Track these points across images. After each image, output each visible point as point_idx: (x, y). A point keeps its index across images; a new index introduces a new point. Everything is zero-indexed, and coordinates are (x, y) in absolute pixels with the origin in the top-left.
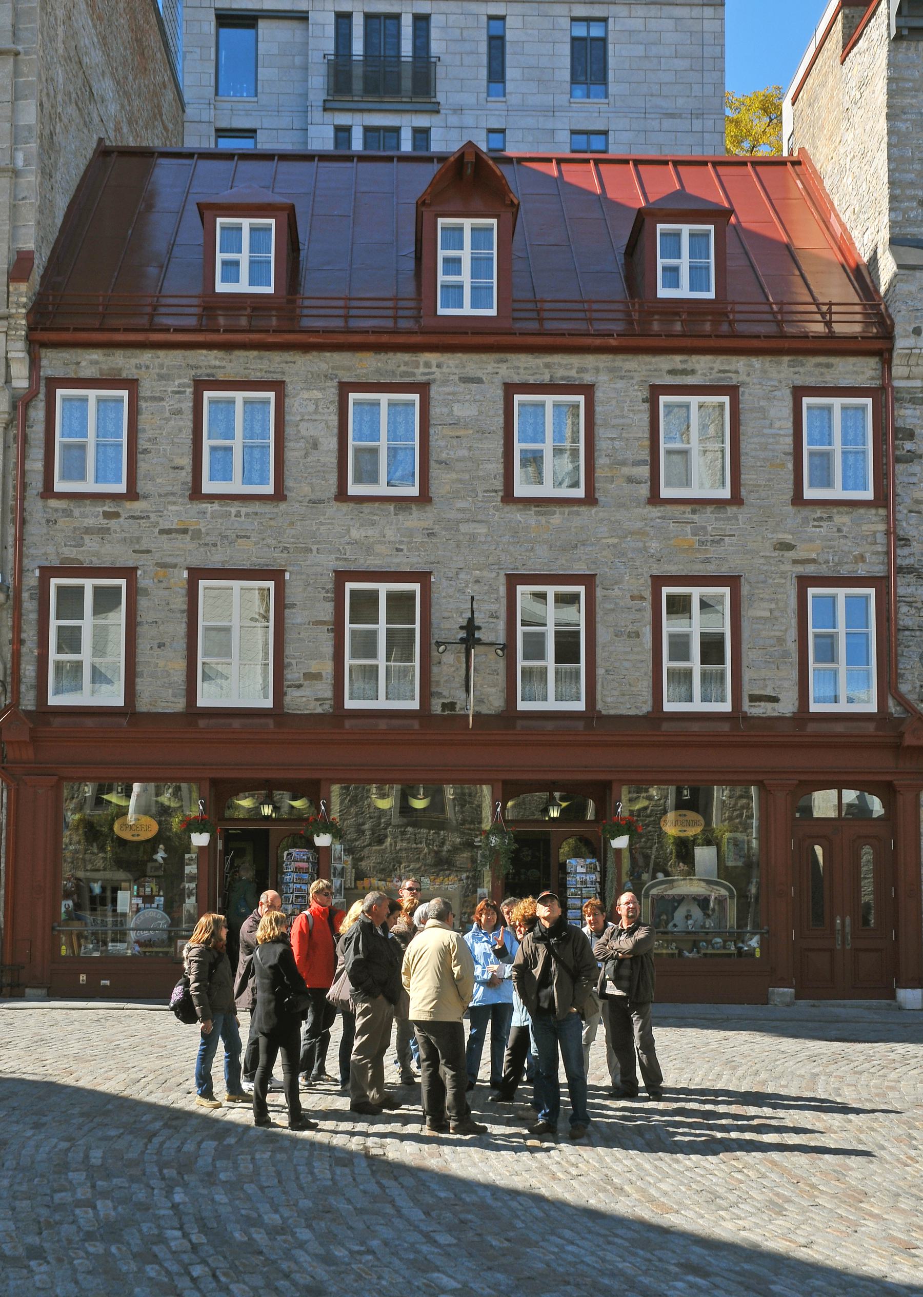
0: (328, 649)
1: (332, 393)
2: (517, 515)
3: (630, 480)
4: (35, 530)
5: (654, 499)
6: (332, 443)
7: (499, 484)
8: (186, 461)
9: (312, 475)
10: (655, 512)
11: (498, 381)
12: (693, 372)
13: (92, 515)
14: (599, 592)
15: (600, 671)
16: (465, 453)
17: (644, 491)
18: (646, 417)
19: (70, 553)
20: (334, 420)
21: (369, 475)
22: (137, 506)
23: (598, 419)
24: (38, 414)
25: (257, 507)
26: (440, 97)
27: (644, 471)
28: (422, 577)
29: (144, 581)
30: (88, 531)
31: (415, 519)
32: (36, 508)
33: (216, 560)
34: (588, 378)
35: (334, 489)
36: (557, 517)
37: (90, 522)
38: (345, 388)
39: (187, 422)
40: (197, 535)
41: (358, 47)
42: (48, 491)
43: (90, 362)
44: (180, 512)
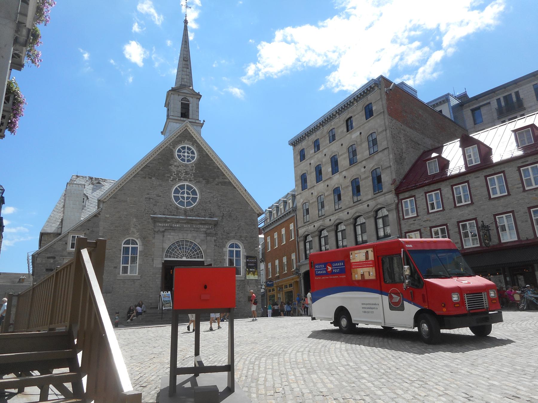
0: (459, 237)
1: (450, 187)
2: (493, 202)
3: (518, 188)
4: (403, 226)
5: (524, 190)
6: (452, 197)
7: (488, 196)
8: (426, 207)
9: (449, 204)
10: (525, 194)
11: (483, 176)
12: (527, 161)
13: (411, 221)
14: (516, 214)
15: (519, 231)
16: (478, 192)
17: (522, 189)
18: (518, 174)
19: (409, 228)
20: (451, 192)
21: (460, 201)
22: (420, 217)
23: (507, 177)
24: (400, 206)
25: (440, 213)
26: (525, 106)
27: (521, 185)
28: (475, 219)
29: (422, 231)
30: (411, 224)
31: (471, 208)
32: (402, 222)
33: (434, 224)
34: (503, 169)
35: (454, 206)
36: (502, 200)
37: (411, 222)
38: (452, 186)
39: (425, 200)
40: (430, 220)
41: (503, 104)
42: (404, 219)
43: (407, 194)
44: (426, 217)
